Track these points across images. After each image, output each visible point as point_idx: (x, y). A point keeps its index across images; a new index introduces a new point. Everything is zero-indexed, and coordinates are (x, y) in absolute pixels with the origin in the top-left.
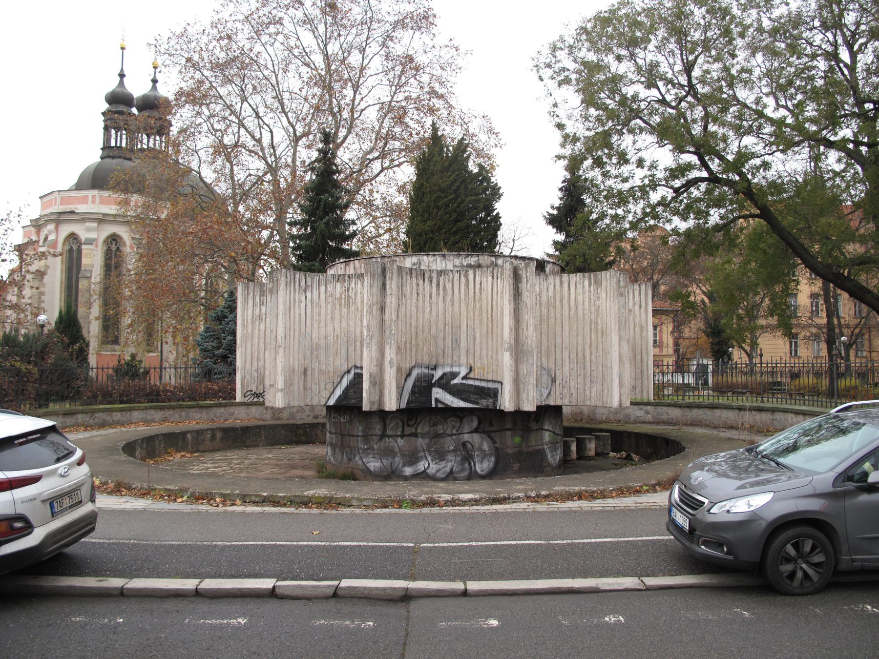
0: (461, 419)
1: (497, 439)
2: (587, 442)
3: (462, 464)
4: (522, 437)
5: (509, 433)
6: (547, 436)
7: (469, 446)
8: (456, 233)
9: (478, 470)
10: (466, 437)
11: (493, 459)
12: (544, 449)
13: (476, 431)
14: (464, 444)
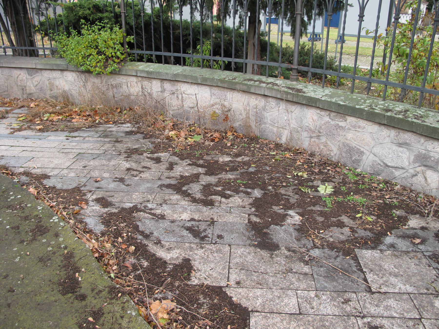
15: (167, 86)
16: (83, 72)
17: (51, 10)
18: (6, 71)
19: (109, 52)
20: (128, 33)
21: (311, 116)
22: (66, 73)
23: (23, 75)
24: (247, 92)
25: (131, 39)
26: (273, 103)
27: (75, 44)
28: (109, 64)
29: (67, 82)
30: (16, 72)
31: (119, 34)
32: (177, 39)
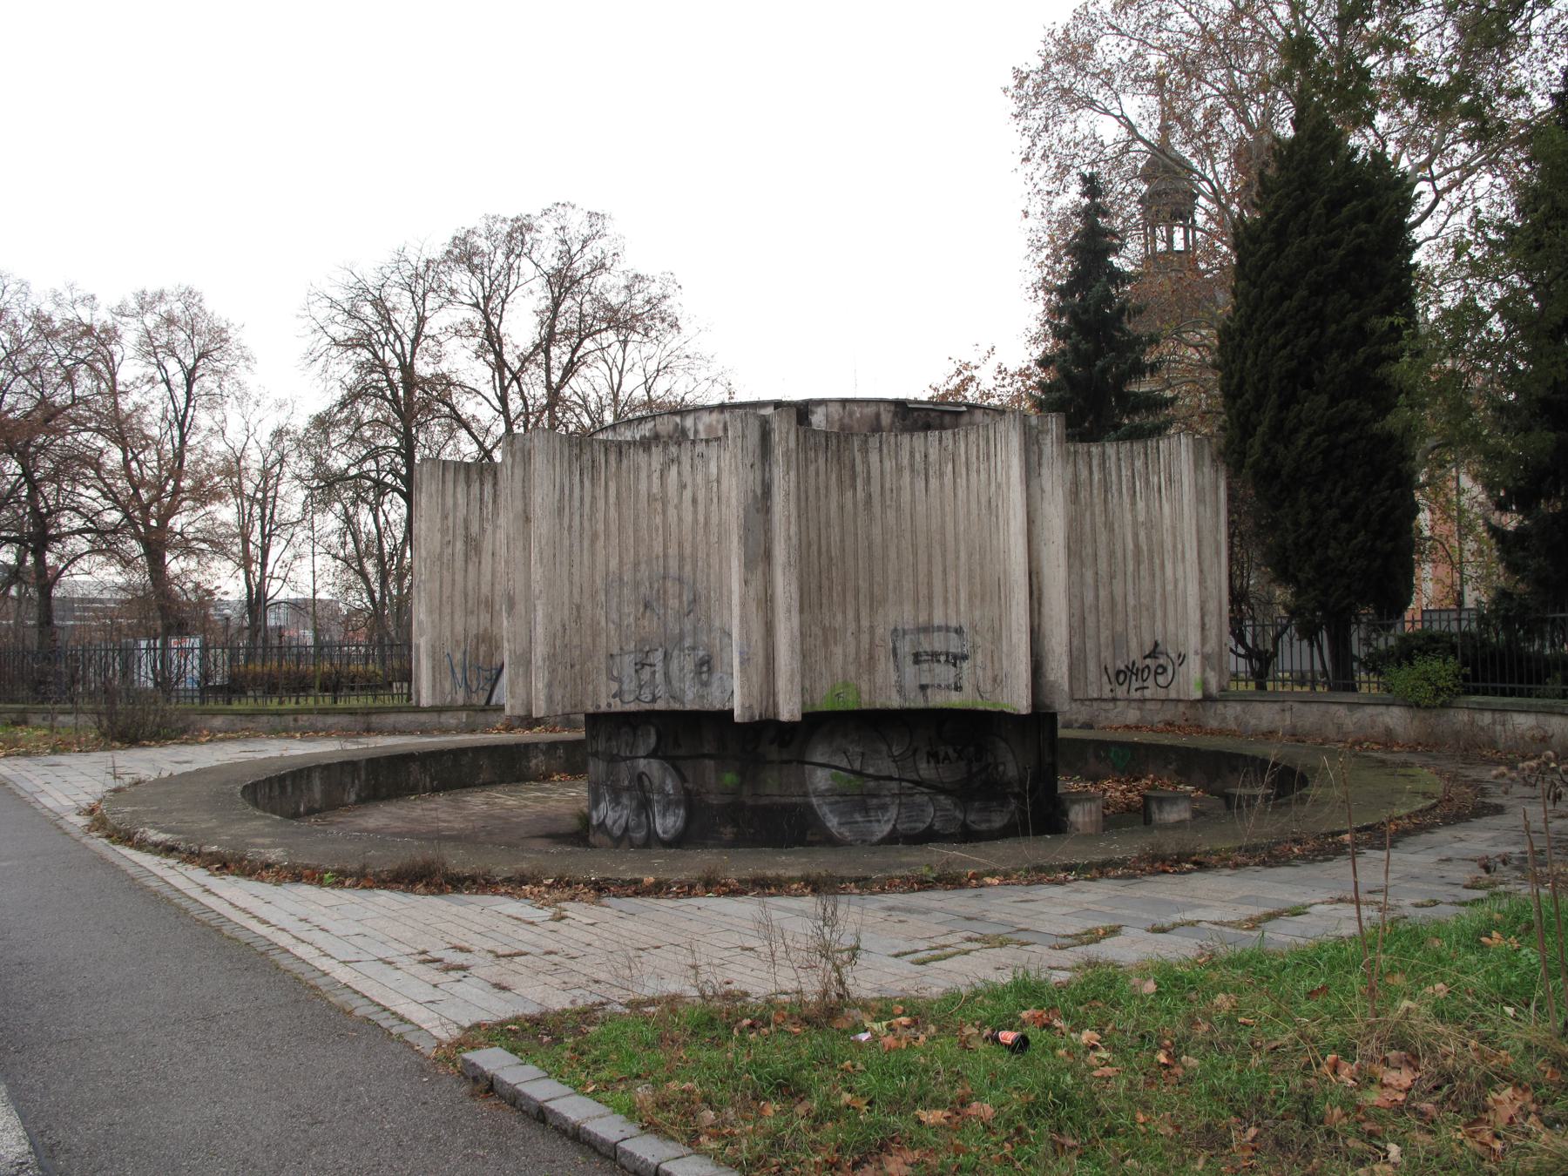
2: (1154, 807)
3: (638, 816)
5: (710, 763)
6: (821, 779)
7: (646, 783)
8: (1279, 325)
9: (659, 830)
11: (682, 812)
12: (810, 806)
13: (652, 755)
14: (640, 776)
15: (1497, 715)
16: (1411, 706)
17: (1382, 640)
18: (1323, 707)
19: (1441, 683)
20: (1465, 664)
23: (1341, 711)
25: (1468, 670)
27: (1403, 677)
28: (1441, 698)
29: (1395, 718)
30: (1334, 708)
31: (1453, 664)
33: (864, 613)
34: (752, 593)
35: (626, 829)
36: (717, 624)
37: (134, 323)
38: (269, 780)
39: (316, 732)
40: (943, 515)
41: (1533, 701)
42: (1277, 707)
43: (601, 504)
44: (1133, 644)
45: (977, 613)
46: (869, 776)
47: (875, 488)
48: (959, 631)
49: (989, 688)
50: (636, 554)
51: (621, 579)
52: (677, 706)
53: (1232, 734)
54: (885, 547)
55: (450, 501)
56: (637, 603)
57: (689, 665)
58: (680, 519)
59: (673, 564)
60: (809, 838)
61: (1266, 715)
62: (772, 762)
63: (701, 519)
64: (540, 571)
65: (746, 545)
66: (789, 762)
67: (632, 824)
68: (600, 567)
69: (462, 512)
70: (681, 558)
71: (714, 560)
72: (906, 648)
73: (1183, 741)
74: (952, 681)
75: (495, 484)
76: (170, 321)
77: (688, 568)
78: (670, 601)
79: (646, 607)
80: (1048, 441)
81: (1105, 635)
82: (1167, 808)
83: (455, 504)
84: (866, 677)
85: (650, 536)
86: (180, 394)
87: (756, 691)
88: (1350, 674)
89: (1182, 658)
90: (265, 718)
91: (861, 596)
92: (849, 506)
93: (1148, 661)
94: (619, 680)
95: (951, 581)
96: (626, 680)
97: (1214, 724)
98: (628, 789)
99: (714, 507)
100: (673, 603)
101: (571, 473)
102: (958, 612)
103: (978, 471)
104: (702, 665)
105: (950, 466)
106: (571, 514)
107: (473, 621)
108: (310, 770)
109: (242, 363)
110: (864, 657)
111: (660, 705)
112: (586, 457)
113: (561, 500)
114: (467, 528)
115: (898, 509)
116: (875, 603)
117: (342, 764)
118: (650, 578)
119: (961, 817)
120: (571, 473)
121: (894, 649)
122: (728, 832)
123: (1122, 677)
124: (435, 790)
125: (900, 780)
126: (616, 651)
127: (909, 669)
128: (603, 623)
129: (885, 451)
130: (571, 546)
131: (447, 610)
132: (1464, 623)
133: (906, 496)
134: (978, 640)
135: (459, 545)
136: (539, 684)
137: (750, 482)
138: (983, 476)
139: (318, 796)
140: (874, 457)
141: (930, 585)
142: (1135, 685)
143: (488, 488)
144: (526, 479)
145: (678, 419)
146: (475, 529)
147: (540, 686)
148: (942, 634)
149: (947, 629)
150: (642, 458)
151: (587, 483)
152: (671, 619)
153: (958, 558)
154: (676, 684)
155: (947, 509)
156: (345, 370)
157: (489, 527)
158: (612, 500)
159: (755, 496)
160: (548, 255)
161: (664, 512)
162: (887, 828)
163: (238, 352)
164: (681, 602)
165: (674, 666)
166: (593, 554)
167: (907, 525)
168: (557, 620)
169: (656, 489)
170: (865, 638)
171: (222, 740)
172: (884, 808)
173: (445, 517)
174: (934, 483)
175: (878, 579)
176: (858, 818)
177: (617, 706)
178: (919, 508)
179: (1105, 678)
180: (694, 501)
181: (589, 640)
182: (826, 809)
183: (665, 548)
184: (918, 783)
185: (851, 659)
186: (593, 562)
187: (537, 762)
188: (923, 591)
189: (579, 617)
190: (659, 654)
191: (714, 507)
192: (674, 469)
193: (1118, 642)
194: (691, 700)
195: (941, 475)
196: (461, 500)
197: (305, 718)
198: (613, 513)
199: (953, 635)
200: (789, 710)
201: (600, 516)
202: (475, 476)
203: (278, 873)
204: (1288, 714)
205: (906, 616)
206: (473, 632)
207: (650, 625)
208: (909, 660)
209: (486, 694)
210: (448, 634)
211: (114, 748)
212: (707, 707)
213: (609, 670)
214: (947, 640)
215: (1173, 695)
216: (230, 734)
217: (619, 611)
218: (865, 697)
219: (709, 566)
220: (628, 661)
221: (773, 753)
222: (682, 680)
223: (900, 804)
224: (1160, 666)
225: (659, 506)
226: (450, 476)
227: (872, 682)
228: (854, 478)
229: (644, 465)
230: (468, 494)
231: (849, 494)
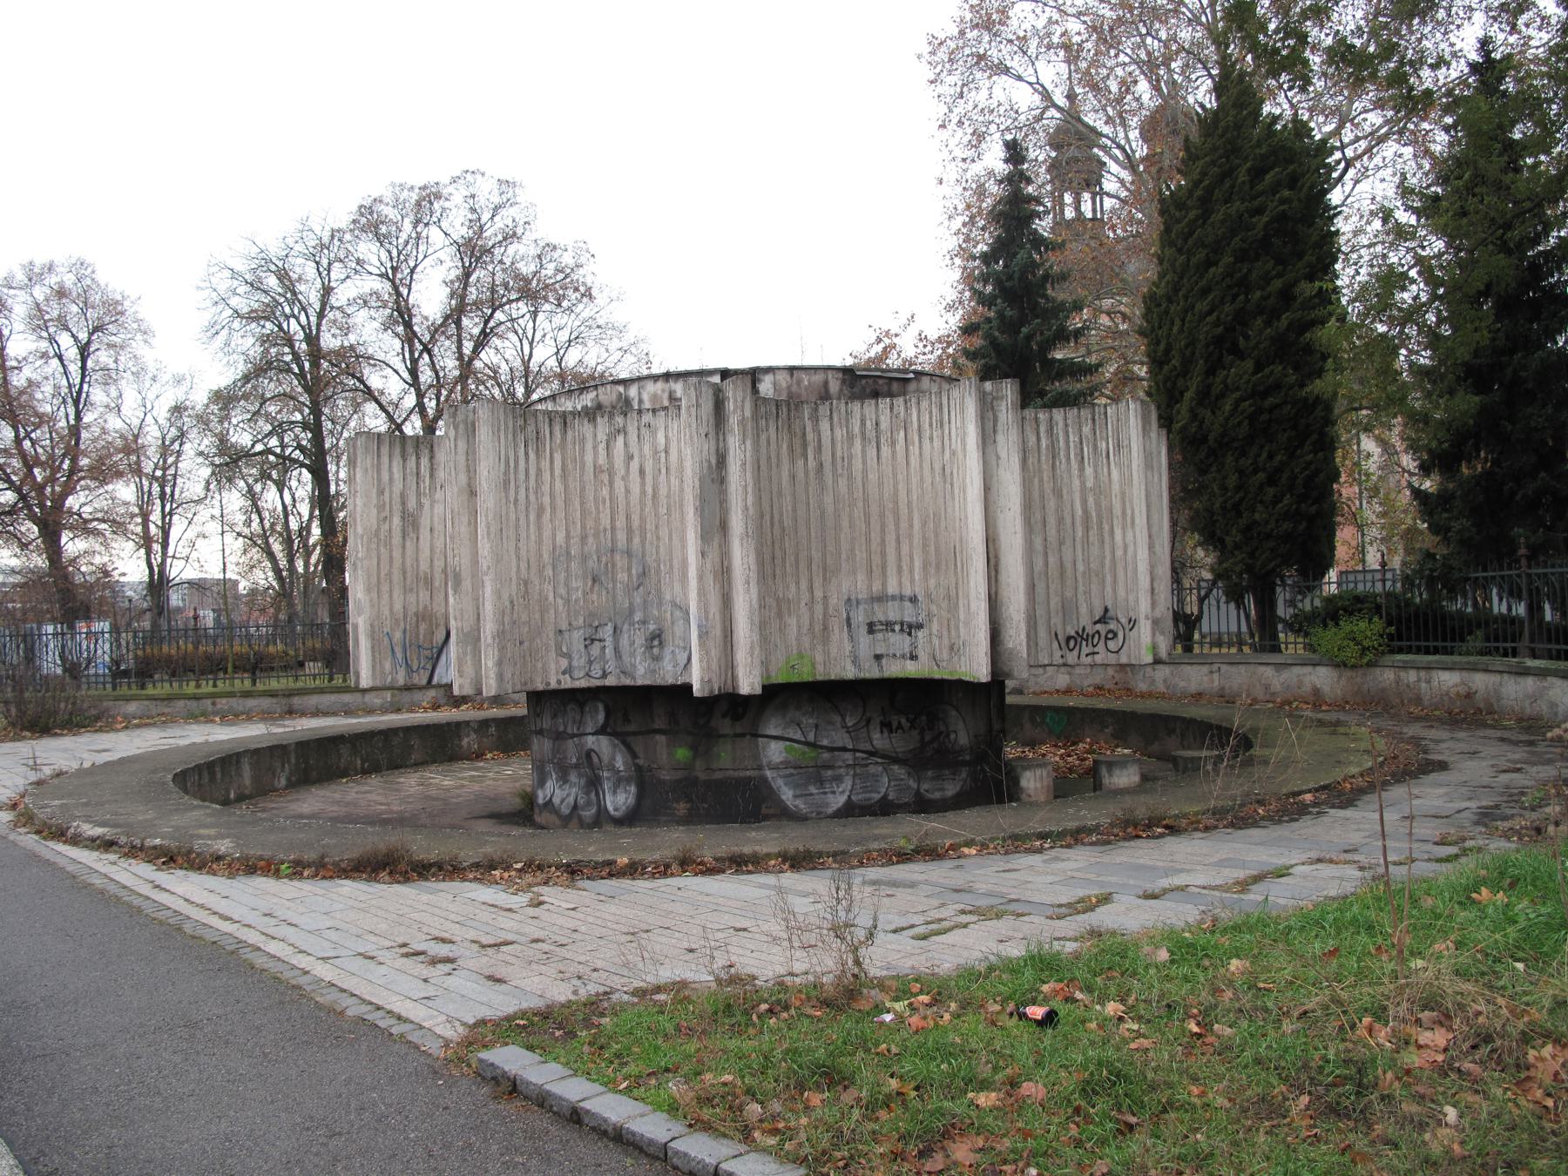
0: (582, 705)
1: (639, 749)
2: (1104, 771)
3: (587, 793)
4: (694, 748)
5: (661, 739)
6: (775, 752)
7: (595, 759)
8: (1205, 292)
9: (610, 808)
10: (590, 741)
11: (633, 789)
12: (765, 780)
13: (601, 731)
14: (589, 753)
15: (1422, 674)
16: (1337, 666)
17: (1307, 601)
18: (1251, 668)
19: (1366, 643)
20: (1390, 624)
21: (1530, 683)
22: (1318, 669)
23: (1269, 672)
24: (1486, 671)
25: (1392, 629)
26: (1506, 677)
27: (1329, 637)
28: (1368, 658)
29: (1322, 678)
30: (1262, 669)
31: (1378, 624)
32: (1453, 630)
33: (817, 584)
34: (709, 566)
35: (575, 807)
36: (668, 597)
37: (22, 296)
38: (198, 768)
39: (236, 715)
40: (896, 484)
41: (1456, 658)
42: (1205, 669)
43: (547, 476)
44: (1084, 610)
45: (932, 582)
46: (822, 747)
47: (826, 457)
48: (913, 600)
49: (945, 656)
50: (583, 527)
51: (568, 553)
52: (628, 682)
53: (1162, 696)
54: (837, 516)
55: (385, 476)
56: (585, 577)
57: (640, 640)
58: (627, 491)
59: (621, 537)
60: (764, 811)
61: (1195, 677)
62: (725, 736)
63: (649, 490)
64: (488, 546)
65: (702, 516)
66: (743, 735)
67: (581, 802)
68: (547, 542)
69: (398, 486)
70: (630, 530)
71: (664, 533)
72: (860, 617)
73: (1117, 705)
74: (907, 650)
75: (432, 458)
76: (61, 293)
77: (636, 540)
78: (620, 571)
79: (594, 581)
80: (1003, 408)
81: (1055, 602)
82: (1117, 772)
83: (391, 480)
84: (820, 648)
85: (597, 509)
86: (74, 369)
87: (714, 666)
88: (1275, 637)
89: (1133, 623)
90: (181, 703)
91: (814, 567)
92: (801, 475)
93: (1098, 627)
94: (568, 656)
95: (905, 549)
96: (575, 656)
97: (1143, 687)
98: (576, 766)
99: (663, 477)
100: (622, 576)
101: (516, 445)
102: (912, 581)
103: (931, 439)
104: (653, 639)
105: (902, 434)
106: (517, 487)
107: (412, 598)
108: (238, 754)
109: (139, 337)
110: (818, 628)
111: (611, 681)
112: (531, 428)
113: (506, 473)
114: (403, 503)
115: (850, 477)
116: (828, 573)
117: (272, 749)
118: (598, 551)
119: (914, 785)
120: (516, 445)
121: (848, 619)
122: (682, 808)
123: (1072, 643)
124: (366, 772)
125: (854, 750)
126: (564, 627)
127: (864, 639)
128: (551, 598)
129: (836, 419)
130: (518, 520)
131: (385, 588)
132: (1388, 584)
133: (857, 465)
134: (934, 608)
135: (396, 521)
136: (489, 662)
137: (705, 452)
138: (937, 443)
139: (248, 782)
140: (825, 426)
141: (883, 554)
142: (1085, 650)
143: (424, 461)
144: (471, 453)
145: (621, 389)
146: (412, 504)
147: (490, 664)
148: (896, 603)
149: (902, 598)
150: (587, 428)
151: (532, 456)
152: (619, 593)
153: (911, 526)
154: (626, 658)
155: (900, 477)
156: (247, 343)
157: (426, 502)
158: (558, 472)
159: (710, 466)
160: (457, 224)
161: (611, 483)
162: (842, 800)
163: (135, 326)
164: (630, 575)
165: (624, 641)
166: (539, 528)
167: (859, 494)
168: (505, 596)
169: (602, 460)
170: (819, 608)
171: (138, 726)
172: (838, 779)
173: (381, 492)
174: (886, 450)
175: (830, 548)
176: (813, 789)
177: (567, 683)
178: (871, 476)
179: (1055, 644)
180: (642, 472)
181: (537, 616)
182: (780, 782)
183: (613, 520)
184: (872, 754)
185: (805, 630)
186: (540, 536)
187: (468, 741)
188: (876, 560)
189: (526, 592)
190: (609, 628)
191: (663, 477)
192: (620, 440)
193: (1067, 609)
194: (642, 675)
195: (893, 443)
196: (397, 475)
197: (224, 701)
198: (559, 485)
199: (907, 604)
200: (748, 683)
201: (546, 488)
202: (410, 450)
203: (230, 865)
204: (1216, 676)
205: (860, 585)
206: (412, 609)
207: (599, 599)
208: (864, 629)
209: (427, 674)
210: (387, 612)
211: (24, 738)
212: (659, 682)
213: (558, 647)
214: (902, 609)
215: (1124, 660)
216: (146, 721)
217: (567, 585)
218: (820, 668)
219: (658, 538)
220: (577, 636)
221: (725, 726)
222: (632, 654)
223: (855, 775)
224: (1111, 631)
225: (605, 477)
226: (385, 450)
227: (827, 653)
228: (805, 446)
229: (589, 436)
230: (404, 468)
231: (800, 463)
